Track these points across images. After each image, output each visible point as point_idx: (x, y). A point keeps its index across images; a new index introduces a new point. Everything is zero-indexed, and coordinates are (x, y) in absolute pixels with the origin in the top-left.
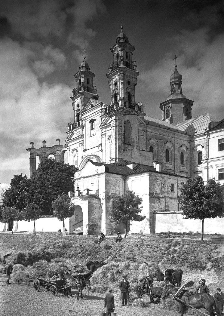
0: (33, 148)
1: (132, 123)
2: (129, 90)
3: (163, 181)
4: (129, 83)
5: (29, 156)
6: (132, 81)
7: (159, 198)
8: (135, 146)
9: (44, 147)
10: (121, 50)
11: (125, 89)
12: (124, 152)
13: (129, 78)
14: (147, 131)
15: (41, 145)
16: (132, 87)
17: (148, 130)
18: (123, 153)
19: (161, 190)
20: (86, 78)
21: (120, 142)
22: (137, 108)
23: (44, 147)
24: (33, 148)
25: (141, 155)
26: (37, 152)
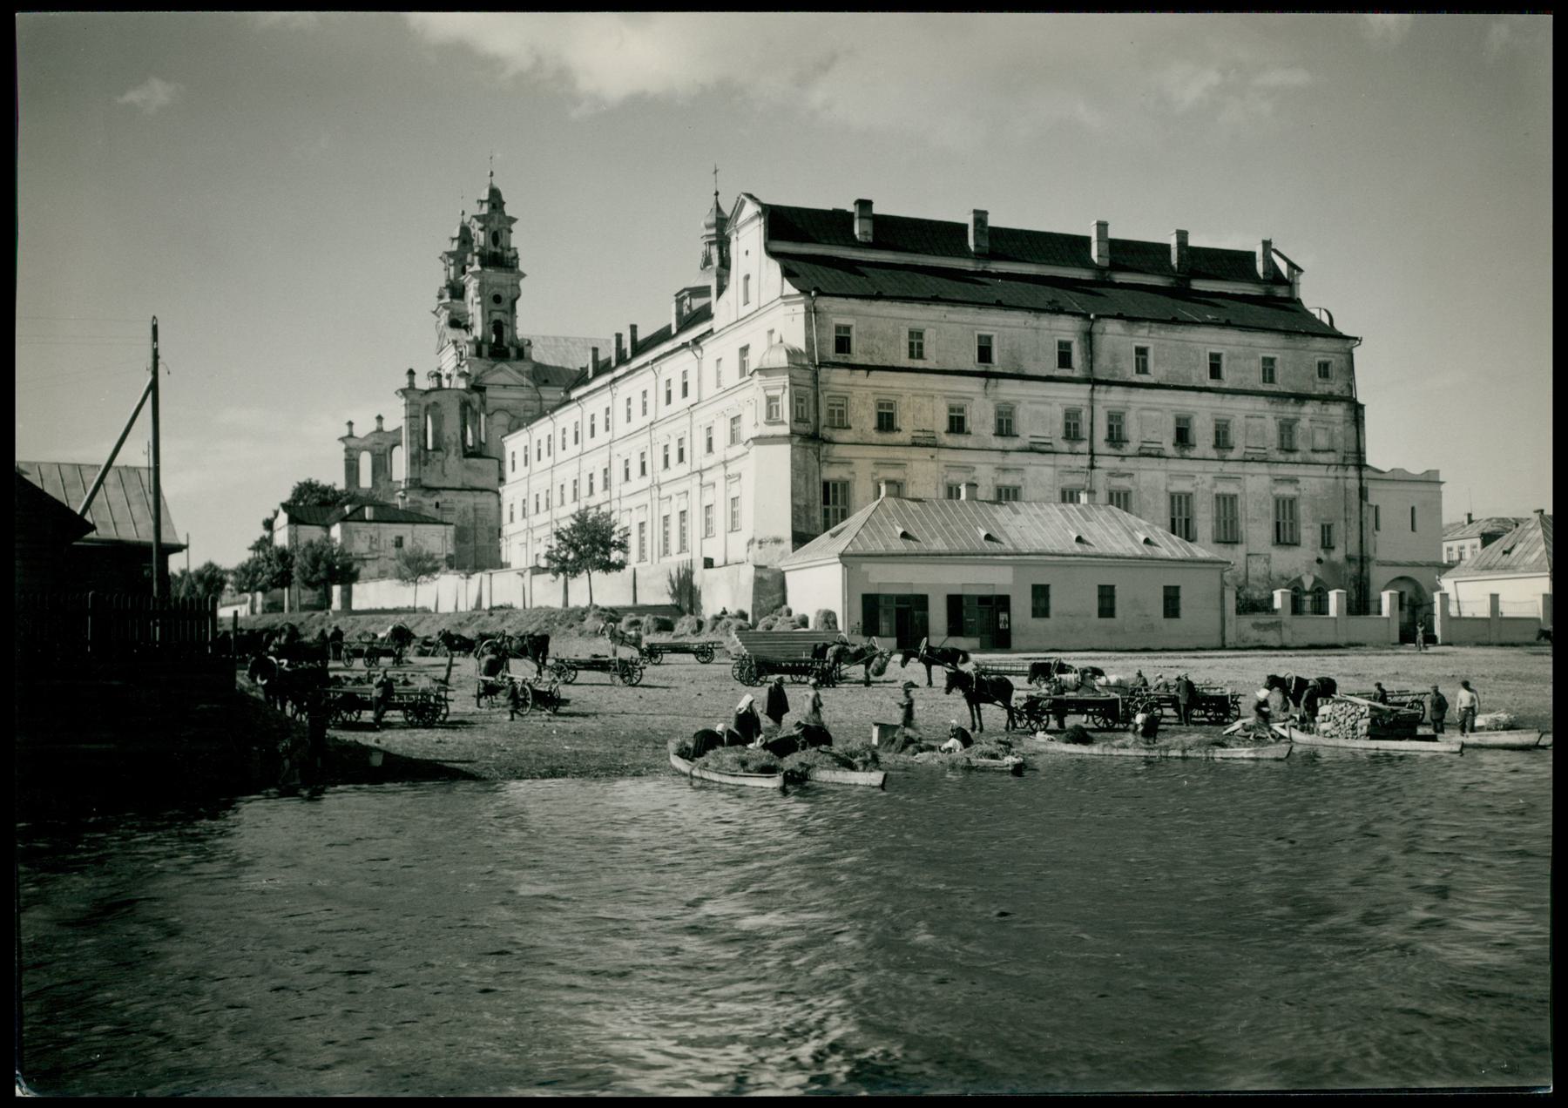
0: (351, 436)
1: (445, 406)
2: (497, 316)
3: (375, 534)
4: (497, 299)
5: (343, 456)
6: (506, 294)
7: (364, 560)
8: (453, 451)
9: (380, 430)
10: (482, 230)
11: (487, 313)
12: (426, 464)
13: (496, 290)
14: (541, 399)
15: (373, 426)
16: (506, 305)
17: (546, 396)
18: (423, 468)
19: (370, 547)
20: (460, 267)
21: (415, 448)
22: (513, 352)
23: (380, 430)
24: (351, 436)
25: (468, 467)
26: (362, 444)
